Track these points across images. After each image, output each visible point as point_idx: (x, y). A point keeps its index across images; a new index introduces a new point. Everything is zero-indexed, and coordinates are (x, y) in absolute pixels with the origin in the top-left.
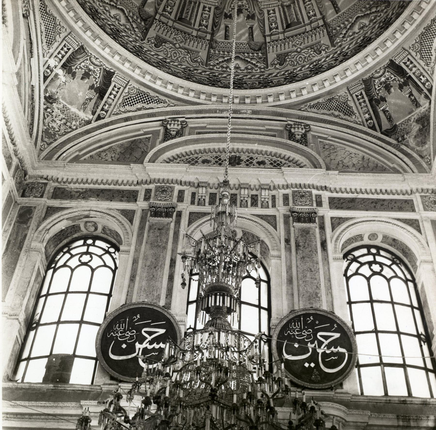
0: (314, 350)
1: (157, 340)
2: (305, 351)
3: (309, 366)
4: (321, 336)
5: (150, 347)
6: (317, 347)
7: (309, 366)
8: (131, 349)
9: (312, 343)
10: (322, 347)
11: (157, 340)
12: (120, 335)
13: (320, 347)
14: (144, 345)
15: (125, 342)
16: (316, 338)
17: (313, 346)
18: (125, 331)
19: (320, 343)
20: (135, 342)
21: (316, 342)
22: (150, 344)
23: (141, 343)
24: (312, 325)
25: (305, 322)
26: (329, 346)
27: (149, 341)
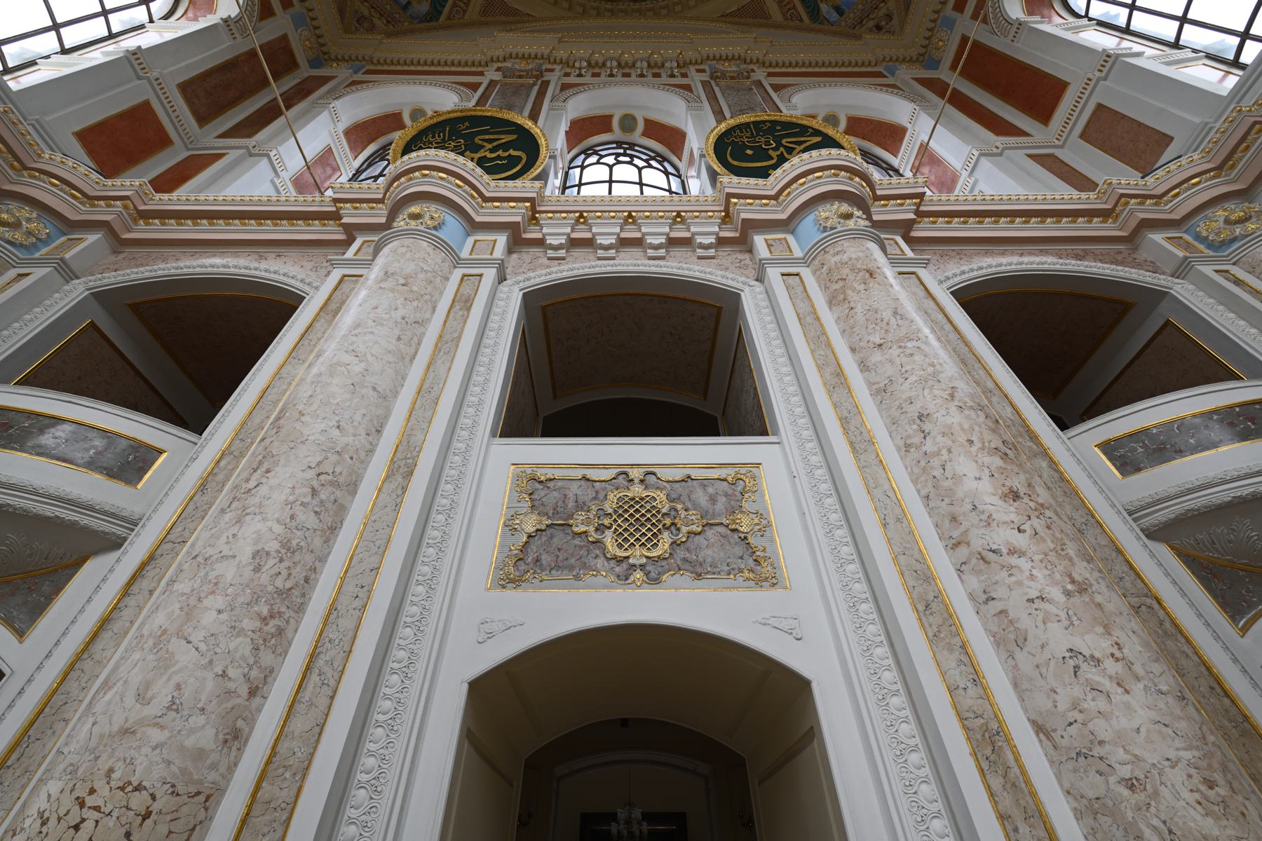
1: (505, 147)
5: (490, 155)
11: (505, 147)
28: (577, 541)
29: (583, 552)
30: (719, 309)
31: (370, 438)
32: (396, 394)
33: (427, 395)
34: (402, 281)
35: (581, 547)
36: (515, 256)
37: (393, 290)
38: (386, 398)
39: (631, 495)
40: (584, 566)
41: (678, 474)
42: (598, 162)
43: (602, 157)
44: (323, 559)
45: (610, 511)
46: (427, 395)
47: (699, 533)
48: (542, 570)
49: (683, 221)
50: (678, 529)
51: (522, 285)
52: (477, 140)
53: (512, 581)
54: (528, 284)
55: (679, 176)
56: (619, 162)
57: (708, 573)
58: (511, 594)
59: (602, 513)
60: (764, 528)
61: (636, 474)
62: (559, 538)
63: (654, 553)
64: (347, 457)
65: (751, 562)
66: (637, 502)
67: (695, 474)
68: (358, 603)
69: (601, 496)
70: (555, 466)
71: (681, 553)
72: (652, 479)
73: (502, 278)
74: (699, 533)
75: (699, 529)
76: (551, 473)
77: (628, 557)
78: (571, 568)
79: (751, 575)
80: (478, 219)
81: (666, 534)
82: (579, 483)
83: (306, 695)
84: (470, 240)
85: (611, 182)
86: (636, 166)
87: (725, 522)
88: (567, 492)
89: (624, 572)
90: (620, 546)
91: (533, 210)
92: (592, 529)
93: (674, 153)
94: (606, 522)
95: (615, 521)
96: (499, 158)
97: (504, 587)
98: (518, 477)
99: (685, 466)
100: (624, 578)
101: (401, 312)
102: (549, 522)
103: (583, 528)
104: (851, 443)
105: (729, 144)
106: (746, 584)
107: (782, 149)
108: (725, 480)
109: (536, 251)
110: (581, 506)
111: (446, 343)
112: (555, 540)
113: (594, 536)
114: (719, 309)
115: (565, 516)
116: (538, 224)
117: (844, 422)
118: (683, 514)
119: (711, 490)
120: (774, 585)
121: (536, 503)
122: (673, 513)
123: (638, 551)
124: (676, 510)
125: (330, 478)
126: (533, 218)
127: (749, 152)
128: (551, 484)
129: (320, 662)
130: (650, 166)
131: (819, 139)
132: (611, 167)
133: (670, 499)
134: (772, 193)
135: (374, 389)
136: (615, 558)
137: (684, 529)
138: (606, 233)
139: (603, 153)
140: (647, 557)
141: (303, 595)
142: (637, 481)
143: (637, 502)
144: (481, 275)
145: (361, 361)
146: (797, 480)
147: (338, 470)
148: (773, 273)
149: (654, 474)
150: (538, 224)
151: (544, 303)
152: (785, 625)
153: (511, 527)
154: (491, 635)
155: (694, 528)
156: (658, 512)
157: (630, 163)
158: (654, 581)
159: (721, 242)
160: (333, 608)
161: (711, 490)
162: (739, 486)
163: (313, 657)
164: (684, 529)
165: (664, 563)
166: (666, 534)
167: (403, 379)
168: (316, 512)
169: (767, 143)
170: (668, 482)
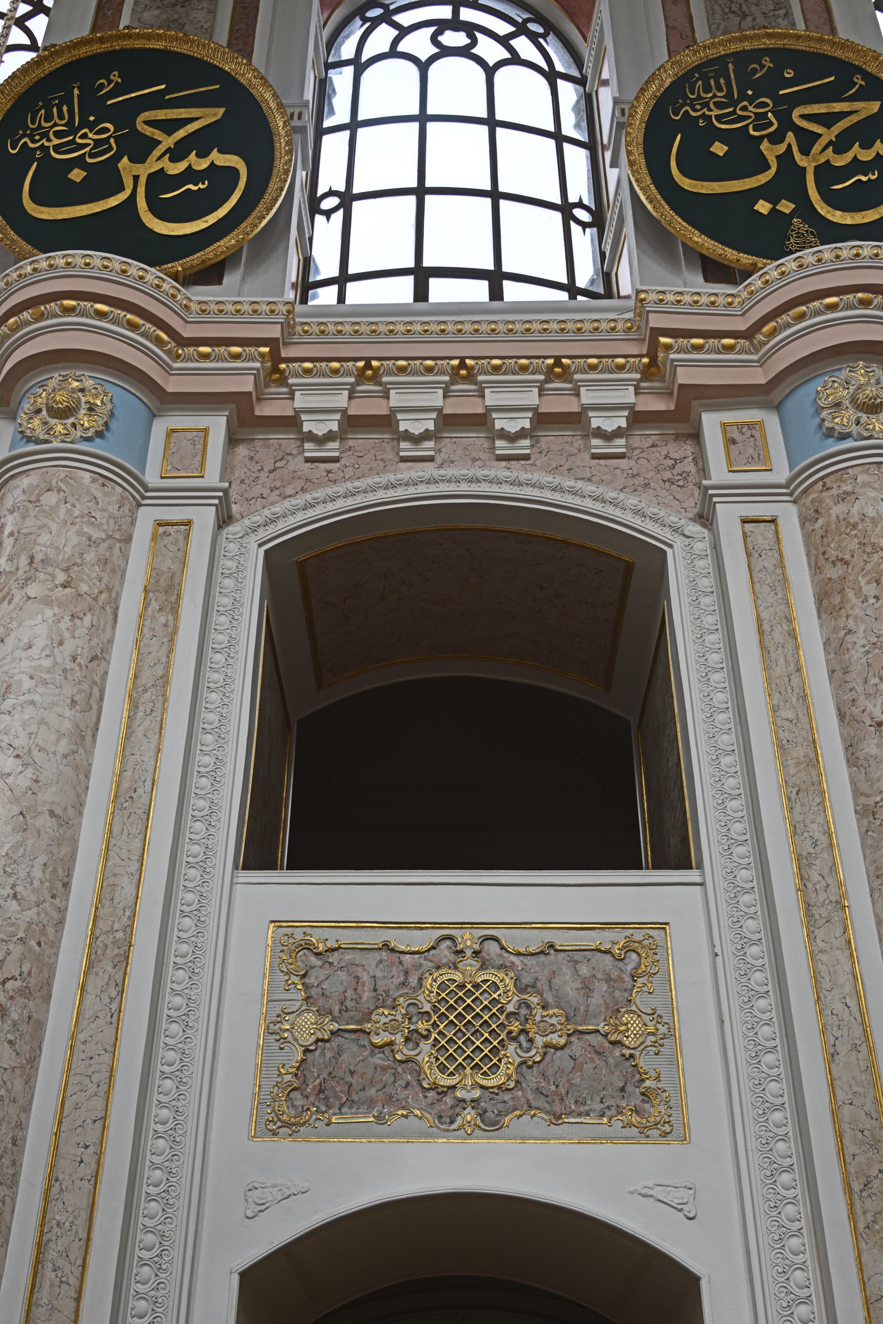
0: (786, 159)
1: (201, 142)
2: (746, 159)
3: (775, 202)
4: (803, 117)
6: (795, 149)
7: (774, 211)
8: (105, 180)
9: (776, 138)
10: (817, 148)
12: (56, 142)
13: (805, 151)
14: (153, 165)
15: (79, 162)
16: (786, 124)
17: (782, 148)
18: (72, 130)
19: (807, 140)
20: (117, 158)
21: (790, 137)
22: (173, 160)
23: (139, 158)
24: (770, 85)
25: (745, 79)
26: (840, 145)
27: (169, 150)
29: (388, 1077)
30: (629, 567)
31: (57, 901)
32: (79, 807)
33: (130, 800)
34: (61, 577)
35: (384, 1069)
36: (242, 451)
37: (47, 602)
38: (67, 820)
39: (458, 977)
40: (390, 1100)
41: (534, 941)
42: (393, 53)
43: (404, 32)
44: (27, 1109)
45: (427, 1007)
46: (130, 800)
47: (562, 1048)
48: (329, 1107)
49: (566, 375)
50: (531, 1041)
51: (262, 534)
52: (141, 127)
53: (288, 1125)
54: (272, 530)
55: (580, 82)
56: (445, 52)
57: (570, 1114)
58: (287, 1148)
59: (415, 1013)
60: (664, 1033)
61: (467, 939)
62: (351, 1054)
63: (492, 1081)
64: (33, 943)
65: (637, 1100)
66: (469, 993)
67: (561, 939)
68: (86, 1171)
69: (413, 980)
71: (532, 1078)
72: (492, 948)
73: (224, 520)
74: (562, 1048)
75: (562, 1041)
76: (334, 937)
77: (453, 1087)
78: (371, 1103)
79: (635, 1119)
80: (172, 386)
81: (512, 1047)
82: (377, 956)
83: (44, 1296)
84: (160, 427)
85: (423, 118)
86: (480, 61)
87: (603, 1028)
88: (360, 972)
89: (446, 1112)
90: (442, 1068)
91: (275, 358)
92: (399, 1039)
93: (572, 17)
94: (422, 1026)
95: (435, 1025)
96: (190, 175)
97: (274, 1133)
98: (279, 946)
99: (545, 926)
100: (447, 1120)
101: (69, 647)
102: (335, 1026)
103: (385, 1037)
104: (808, 906)
105: (677, 127)
106: (627, 1132)
107: (790, 137)
108: (607, 952)
109: (285, 439)
110: (383, 1000)
111: (149, 690)
112: (345, 1056)
114: (629, 567)
115: (359, 1015)
116: (282, 381)
117: (803, 862)
118: (539, 1012)
119: (584, 970)
120: (665, 1134)
121: (314, 992)
122: (524, 1011)
123: (469, 1077)
124: (528, 1006)
125: (18, 984)
126: (275, 372)
127: (719, 149)
128: (334, 958)
129: (52, 1254)
130: (515, 59)
131: (875, 106)
132: (423, 67)
133: (522, 989)
134: (742, 325)
135: (52, 813)
136: (434, 1087)
137: (539, 1041)
138: (417, 403)
139: (405, 19)
140: (482, 1087)
141: (14, 1163)
142: (469, 953)
143: (469, 993)
144: (188, 523)
145: (25, 765)
146: (719, 959)
147: (26, 968)
148: (728, 515)
149: (496, 939)
150: (282, 381)
151: (302, 557)
152: (675, 1197)
153: (274, 1032)
155: (554, 1039)
156: (501, 1010)
157: (465, 52)
158: (491, 1124)
159: (638, 418)
160: (52, 1178)
161: (584, 970)
162: (637, 952)
163: (41, 1247)
164: (539, 1041)
165: (507, 1097)
166: (512, 1047)
167: (87, 776)
168: (10, 1042)
169: (761, 122)
170: (519, 954)
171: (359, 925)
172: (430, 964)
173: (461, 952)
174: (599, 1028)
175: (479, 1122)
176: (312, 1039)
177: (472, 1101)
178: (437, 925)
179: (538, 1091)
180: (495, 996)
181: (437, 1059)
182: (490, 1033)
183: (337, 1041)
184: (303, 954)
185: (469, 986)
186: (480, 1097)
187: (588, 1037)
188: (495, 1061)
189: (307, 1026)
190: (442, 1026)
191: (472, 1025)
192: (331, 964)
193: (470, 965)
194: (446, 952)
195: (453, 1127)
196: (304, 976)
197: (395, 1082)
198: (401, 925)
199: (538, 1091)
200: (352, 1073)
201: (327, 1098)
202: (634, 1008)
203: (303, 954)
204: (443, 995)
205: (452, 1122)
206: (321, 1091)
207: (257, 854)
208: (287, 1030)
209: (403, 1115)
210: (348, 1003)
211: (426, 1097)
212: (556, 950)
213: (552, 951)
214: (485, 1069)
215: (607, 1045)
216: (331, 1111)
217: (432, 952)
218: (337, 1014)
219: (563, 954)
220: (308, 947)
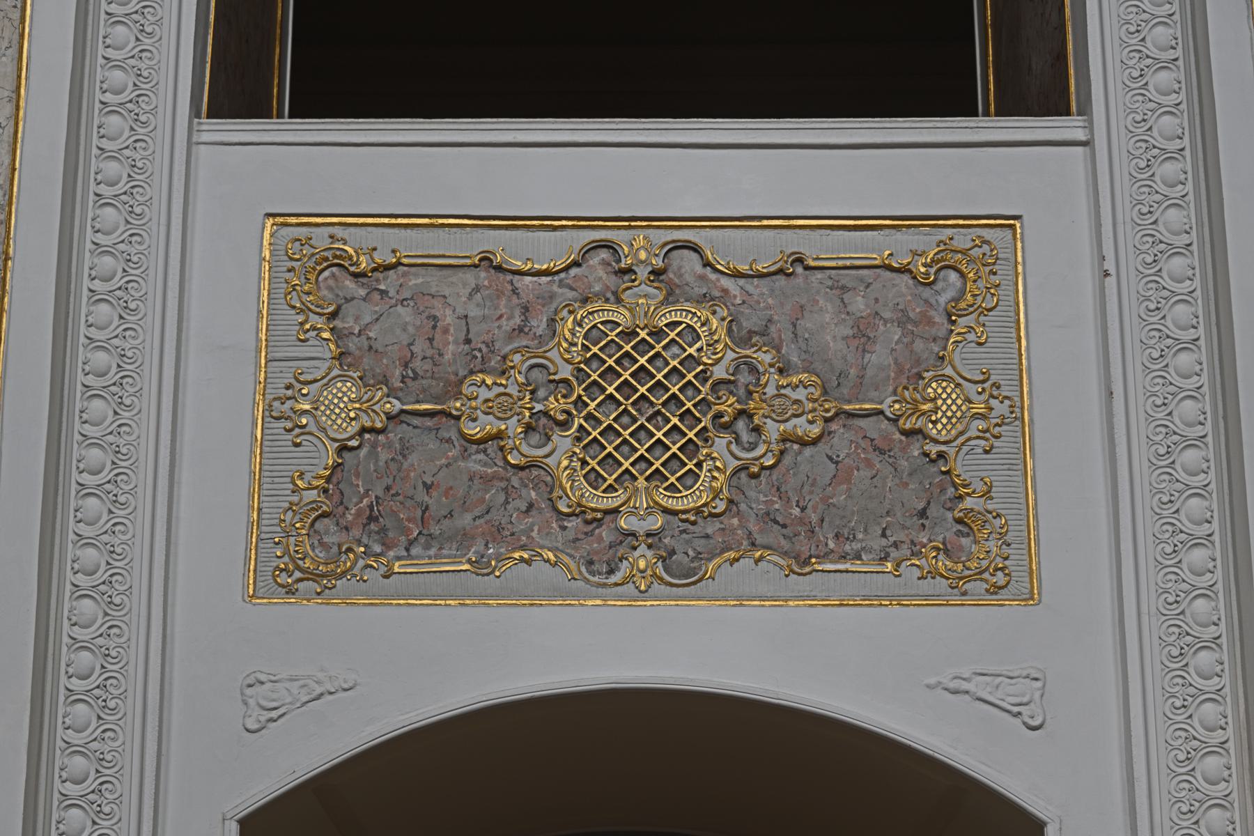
28: (475, 463)
29: (493, 495)
35: (487, 480)
39: (623, 317)
40: (497, 533)
41: (765, 250)
45: (566, 372)
47: (815, 442)
48: (388, 546)
50: (757, 430)
53: (315, 577)
57: (824, 556)
58: (310, 615)
59: (543, 381)
60: (1002, 414)
61: (640, 248)
62: (426, 455)
65: (948, 531)
66: (643, 346)
67: (815, 247)
69: (539, 324)
70: (396, 221)
71: (758, 496)
74: (815, 442)
75: (815, 430)
76: (386, 245)
77: (616, 511)
78: (464, 539)
79: (943, 563)
81: (721, 442)
82: (470, 277)
87: (890, 406)
88: (438, 309)
89: (601, 552)
90: (594, 479)
92: (513, 427)
94: (555, 405)
99: (788, 223)
102: (395, 406)
103: (489, 424)
106: (927, 586)
112: (413, 458)
113: (523, 450)
115: (437, 387)
118: (772, 380)
119: (859, 304)
120: (996, 589)
122: (744, 378)
123: (643, 494)
124: (753, 369)
128: (389, 282)
136: (580, 511)
137: (773, 430)
140: (666, 511)
142: (643, 272)
143: (643, 346)
146: (1111, 282)
149: (695, 248)
152: (1007, 694)
153: (284, 415)
154: (274, 714)
155: (800, 426)
156: (703, 377)
161: (859, 304)
162: (957, 273)
164: (773, 430)
165: (712, 527)
166: (721, 442)
170: (737, 275)
171: (435, 222)
172: (571, 294)
173: (629, 270)
174: (884, 407)
175: (660, 570)
176: (354, 428)
177: (648, 535)
178: (581, 222)
179: (769, 517)
180: (692, 351)
181: (584, 463)
182: (682, 417)
183: (397, 433)
184: (331, 278)
185: (643, 334)
186: (663, 529)
187: (862, 423)
188: (690, 466)
189: (343, 405)
190: (593, 405)
191: (647, 403)
192: (383, 293)
193: (645, 295)
194: (601, 273)
195: (614, 579)
196: (334, 315)
197: (507, 502)
198: (514, 223)
199: (769, 517)
200: (428, 487)
201: (383, 530)
202: (949, 371)
203: (331, 278)
204: (595, 350)
205: (611, 572)
206: (372, 519)
207: (235, 88)
208: (305, 412)
209: (522, 560)
210: (417, 364)
211: (564, 528)
212: (807, 268)
213: (799, 270)
214: (672, 479)
215: (897, 436)
216: (391, 554)
217: (574, 271)
218: (399, 384)
219: (819, 275)
220: (340, 262)
